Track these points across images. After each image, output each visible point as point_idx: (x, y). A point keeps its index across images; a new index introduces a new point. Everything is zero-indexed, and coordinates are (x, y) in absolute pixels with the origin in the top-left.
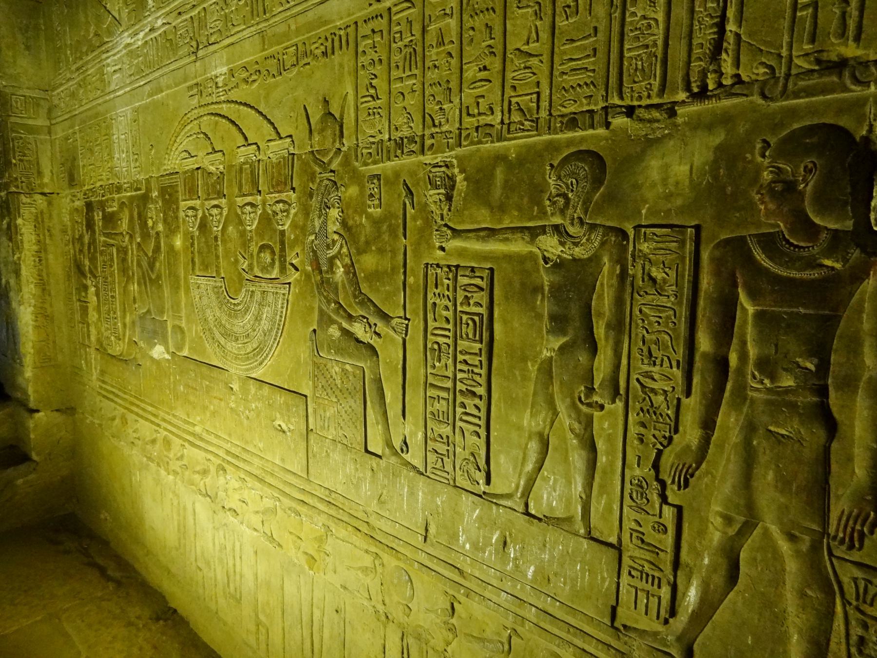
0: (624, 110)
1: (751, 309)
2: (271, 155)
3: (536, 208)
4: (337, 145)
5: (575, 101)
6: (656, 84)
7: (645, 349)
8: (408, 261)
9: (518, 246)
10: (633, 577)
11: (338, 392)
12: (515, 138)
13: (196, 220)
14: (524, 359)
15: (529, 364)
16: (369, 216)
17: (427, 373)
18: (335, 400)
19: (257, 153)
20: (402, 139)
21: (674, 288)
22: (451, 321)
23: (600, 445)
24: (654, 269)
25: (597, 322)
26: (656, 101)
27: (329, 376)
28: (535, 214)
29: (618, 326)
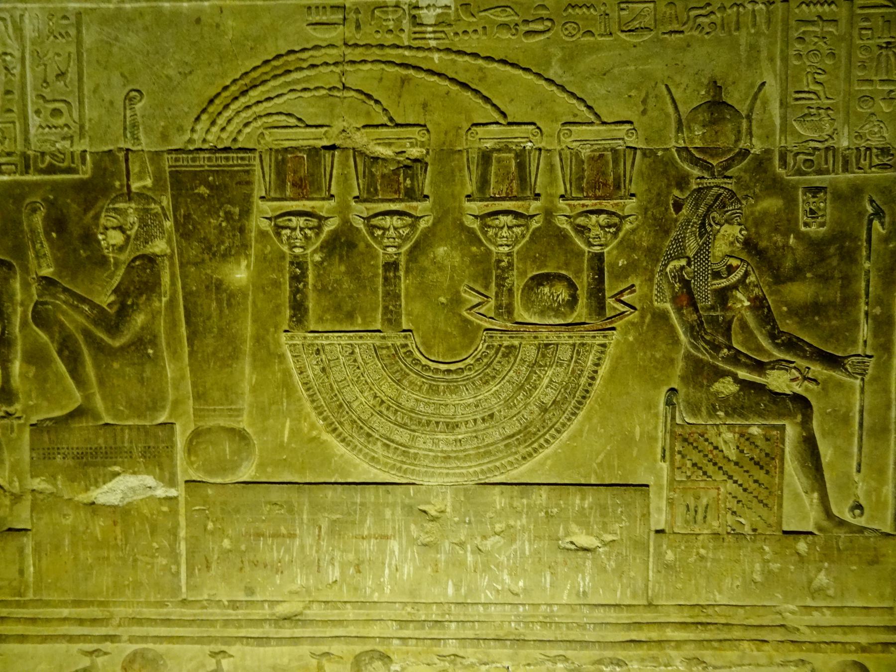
4: (742, 145)
11: (730, 468)
13: (317, 235)
16: (800, 236)
18: (720, 477)
27: (710, 448)
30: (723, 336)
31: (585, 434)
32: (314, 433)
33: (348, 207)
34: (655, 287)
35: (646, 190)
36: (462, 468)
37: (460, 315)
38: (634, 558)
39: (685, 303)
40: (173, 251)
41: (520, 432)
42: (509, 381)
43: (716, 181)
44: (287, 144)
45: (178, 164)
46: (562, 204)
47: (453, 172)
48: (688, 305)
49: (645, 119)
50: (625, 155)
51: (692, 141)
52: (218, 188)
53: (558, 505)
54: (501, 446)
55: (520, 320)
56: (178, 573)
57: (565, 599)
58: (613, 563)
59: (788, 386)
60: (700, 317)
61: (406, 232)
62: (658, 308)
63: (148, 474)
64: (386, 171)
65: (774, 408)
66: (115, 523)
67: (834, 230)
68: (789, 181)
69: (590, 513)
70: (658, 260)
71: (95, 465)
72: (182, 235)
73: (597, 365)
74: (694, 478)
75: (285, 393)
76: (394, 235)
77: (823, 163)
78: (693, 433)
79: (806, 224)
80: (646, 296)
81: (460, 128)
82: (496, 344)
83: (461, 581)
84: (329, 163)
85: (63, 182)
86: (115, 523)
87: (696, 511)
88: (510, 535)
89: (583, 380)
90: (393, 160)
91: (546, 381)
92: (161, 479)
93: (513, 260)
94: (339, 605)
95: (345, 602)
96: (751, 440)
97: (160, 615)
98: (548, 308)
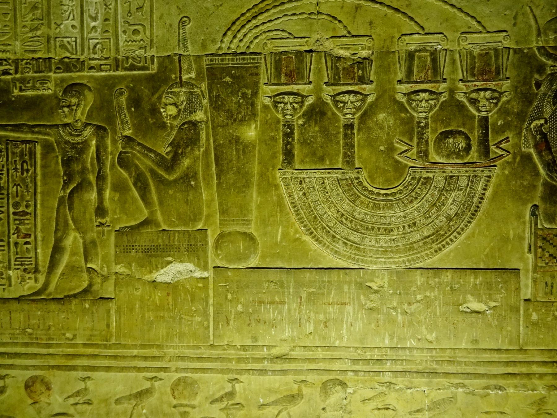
13: (301, 107)
31: (476, 235)
32: (298, 236)
33: (321, 90)
36: (395, 258)
37: (393, 158)
38: (511, 318)
40: (208, 118)
41: (433, 234)
44: (282, 49)
45: (212, 63)
46: (461, 85)
47: (389, 65)
52: (238, 78)
54: (421, 244)
55: (433, 161)
56: (208, 327)
57: (463, 346)
58: (496, 322)
61: (359, 104)
63: (190, 262)
64: (345, 66)
66: (168, 294)
69: (480, 288)
71: (156, 256)
72: (214, 108)
73: (485, 189)
75: (278, 210)
76: (351, 107)
80: (516, 144)
81: (393, 37)
82: (417, 176)
83: (394, 333)
84: (309, 61)
85: (140, 75)
86: (168, 294)
89: (475, 200)
90: (350, 58)
91: (450, 201)
92: (198, 265)
94: (313, 349)
95: (317, 347)
97: (196, 354)
98: (452, 153)
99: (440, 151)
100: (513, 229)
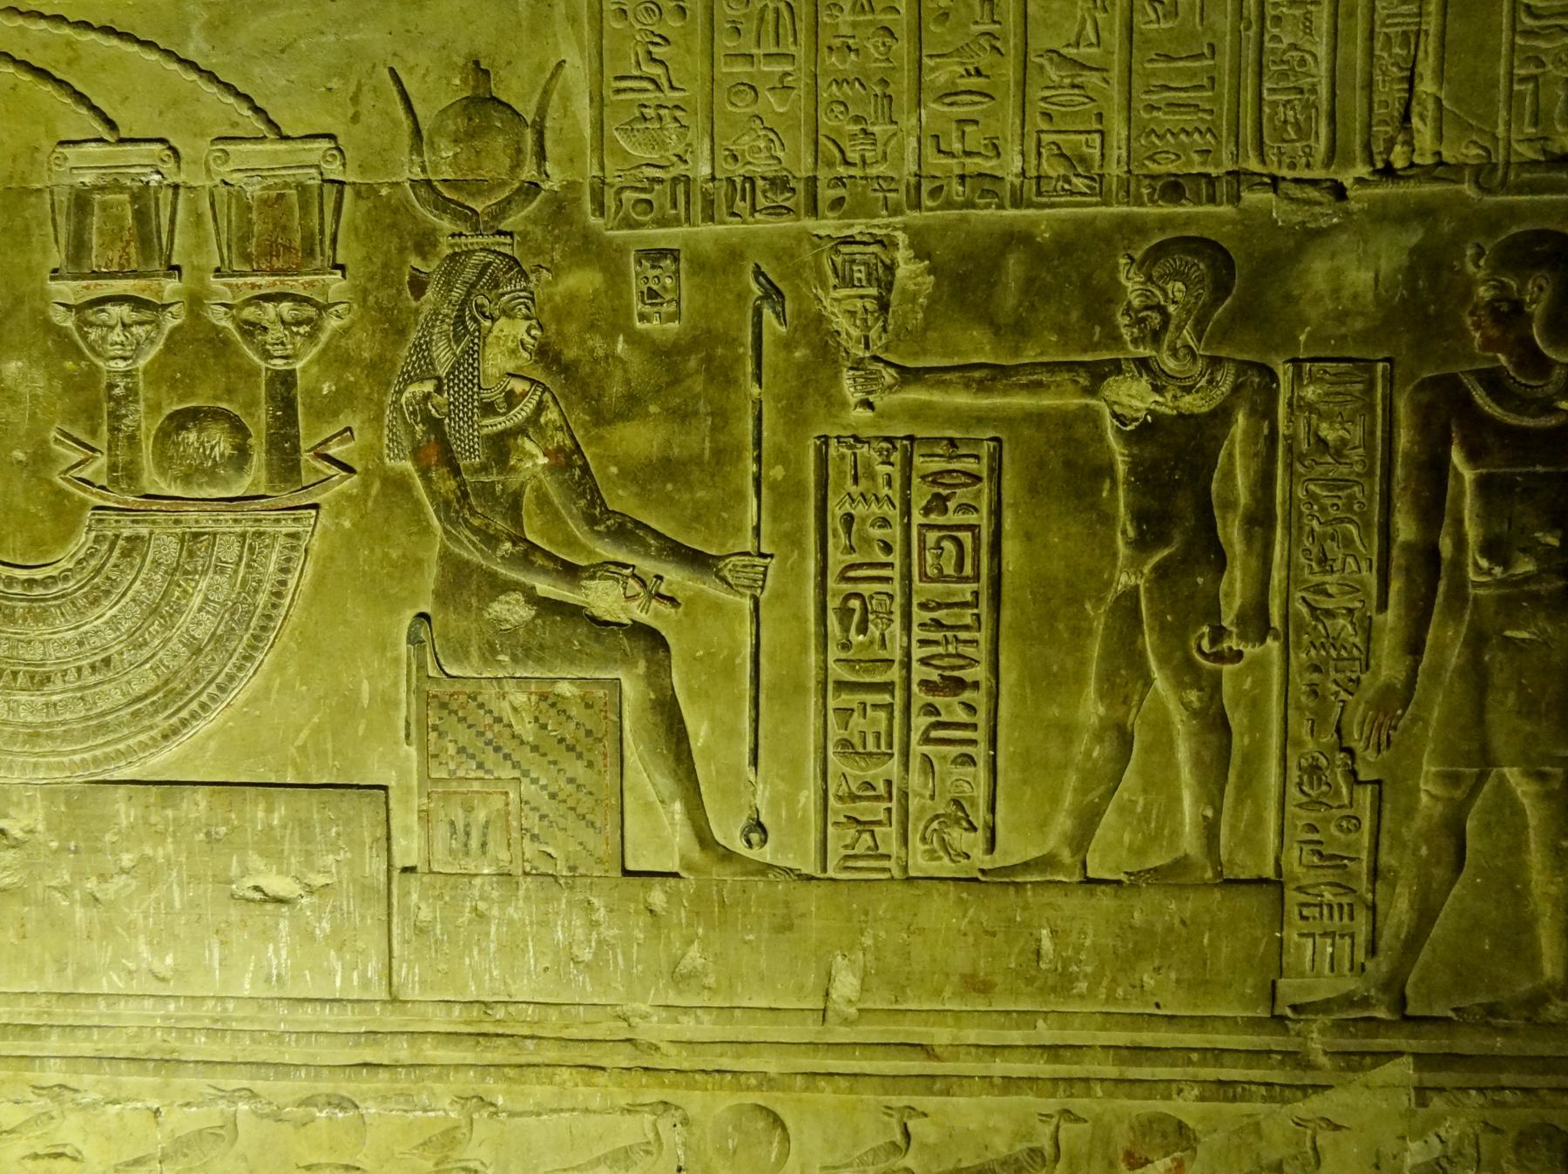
0: (1267, 180)
1: (1468, 475)
2: (235, 178)
3: (1098, 329)
4: (528, 172)
5: (1178, 156)
6: (1322, 146)
7: (1315, 550)
8: (765, 434)
9: (1063, 399)
10: (1307, 918)
11: (524, 755)
12: (1052, 205)
14: (1075, 600)
15: (1088, 606)
16: (635, 339)
17: (825, 661)
18: (507, 772)
19: (171, 164)
20: (751, 180)
21: (1361, 451)
22: (897, 548)
23: (1236, 720)
24: (1324, 425)
25: (1224, 518)
26: (1318, 173)
27: (488, 720)
28: (1096, 338)
29: (1260, 520)
30: (504, 518)
31: (274, 696)
34: (386, 431)
35: (364, 259)
38: (363, 918)
39: (434, 460)
41: (156, 690)
42: (133, 600)
43: (480, 239)
46: (216, 284)
48: (440, 463)
49: (357, 129)
50: (321, 196)
51: (436, 166)
53: (227, 822)
55: (153, 492)
58: (326, 925)
59: (624, 610)
60: (462, 485)
62: (392, 469)
65: (597, 648)
67: (694, 328)
68: (610, 240)
69: (283, 837)
70: (389, 384)
73: (285, 571)
74: (461, 773)
77: (668, 205)
78: (458, 693)
79: (643, 317)
87: (468, 834)
88: (147, 870)
89: (262, 599)
91: (197, 600)
93: (136, 383)
96: (560, 706)
98: (197, 470)
99: (166, 465)
100: (369, 678)
